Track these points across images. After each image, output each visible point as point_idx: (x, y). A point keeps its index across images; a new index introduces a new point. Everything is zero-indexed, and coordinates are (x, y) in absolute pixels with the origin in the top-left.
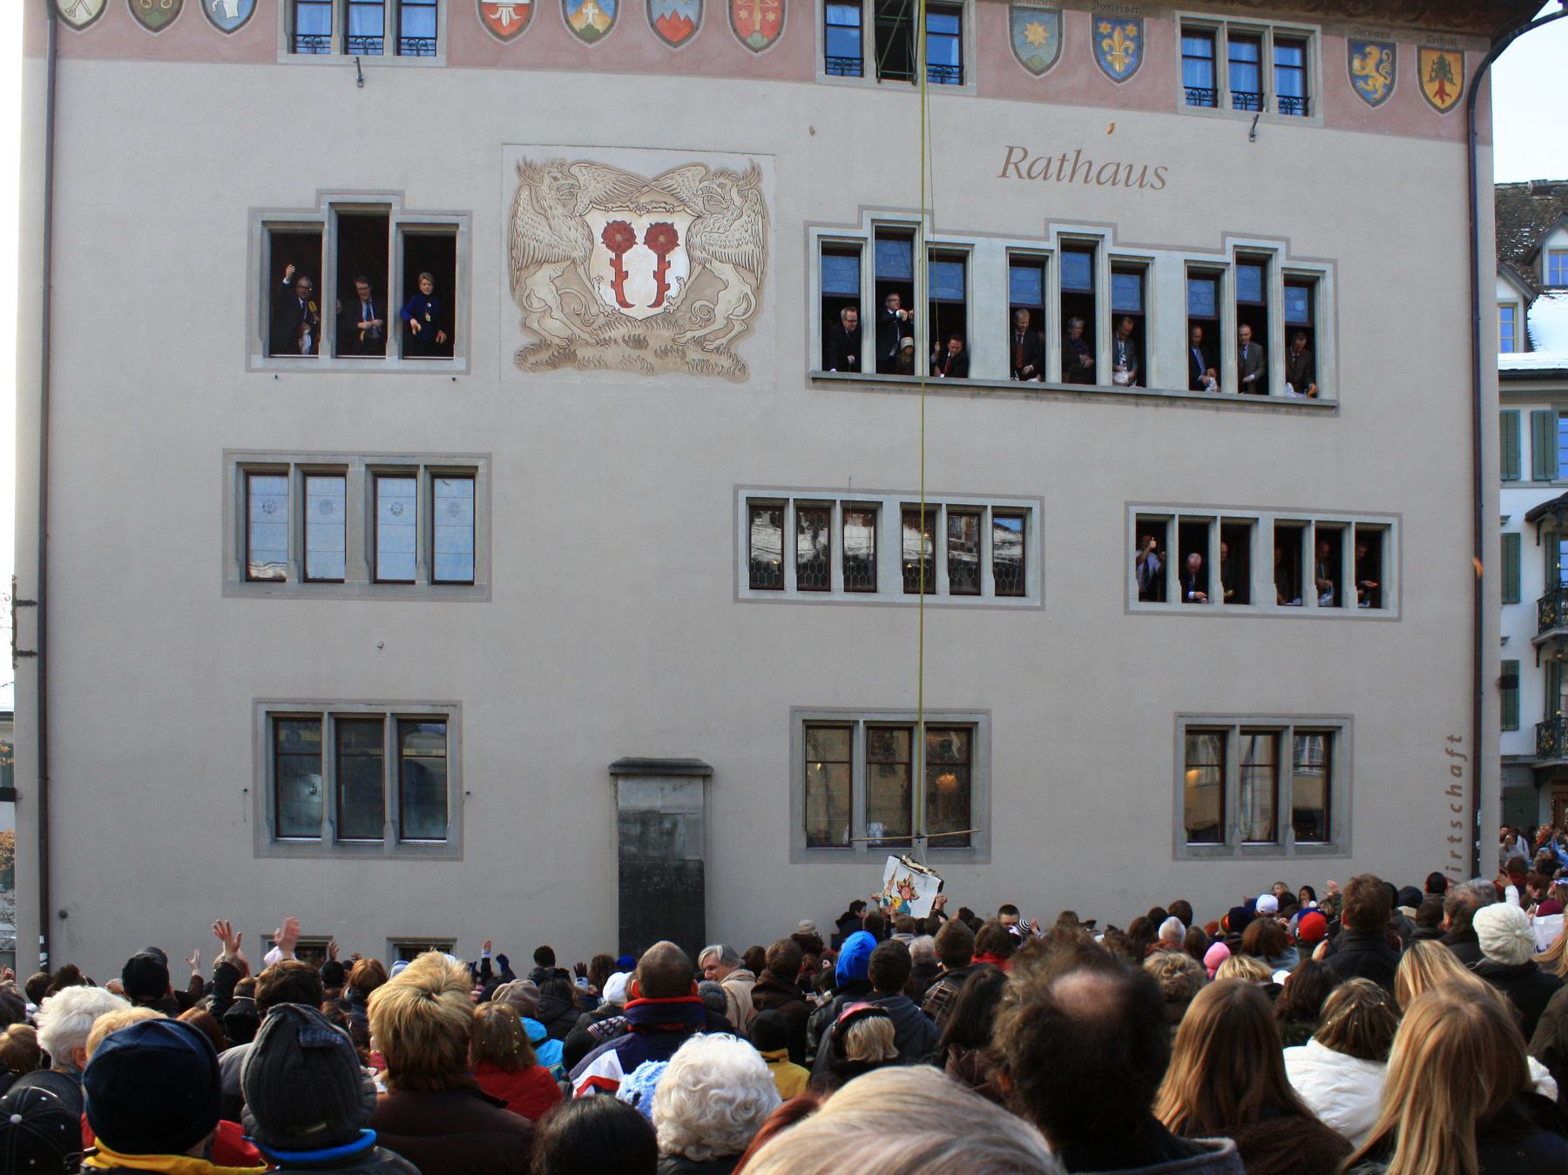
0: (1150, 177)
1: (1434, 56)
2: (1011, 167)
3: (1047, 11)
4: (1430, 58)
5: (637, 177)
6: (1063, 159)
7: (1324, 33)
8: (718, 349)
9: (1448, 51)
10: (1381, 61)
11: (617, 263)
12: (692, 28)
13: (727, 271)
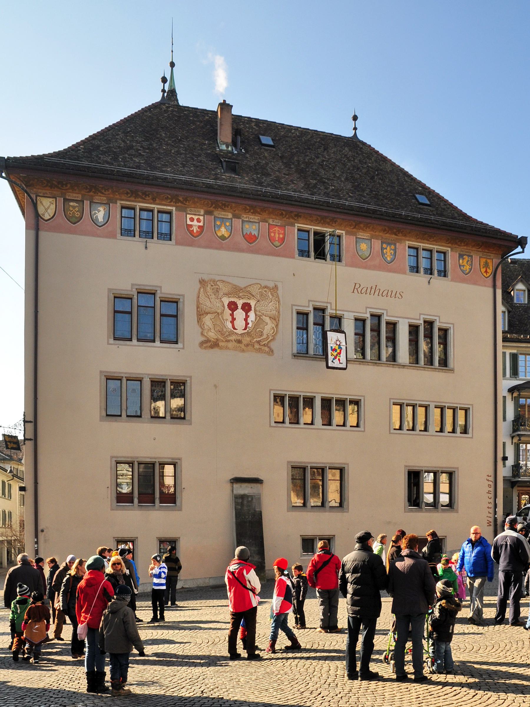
0: (398, 295)
1: (484, 260)
2: (355, 289)
3: (367, 239)
4: (483, 261)
5: (238, 286)
7: (451, 251)
10: (468, 261)
11: (232, 315)
13: (267, 319)
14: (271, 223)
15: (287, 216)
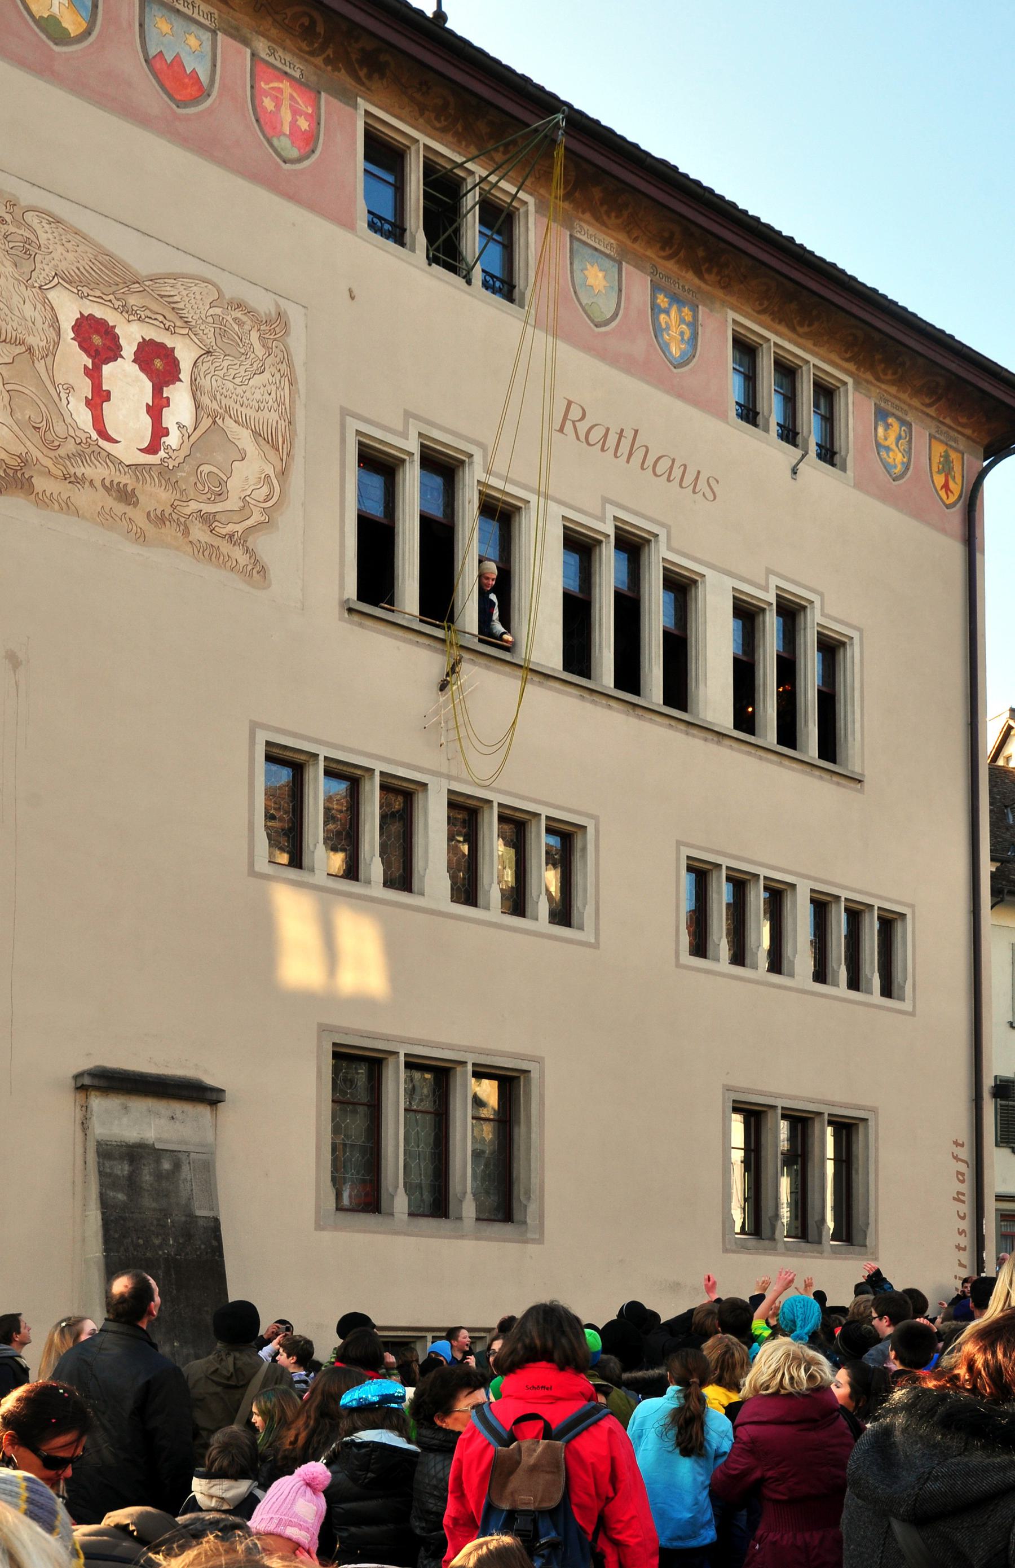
0: (702, 484)
2: (569, 425)
5: (125, 266)
6: (621, 434)
8: (231, 536)
9: (951, 447)
10: (899, 438)
11: (94, 374)
12: (202, 93)
13: (244, 438)
14: (263, 55)
15: (330, 52)
